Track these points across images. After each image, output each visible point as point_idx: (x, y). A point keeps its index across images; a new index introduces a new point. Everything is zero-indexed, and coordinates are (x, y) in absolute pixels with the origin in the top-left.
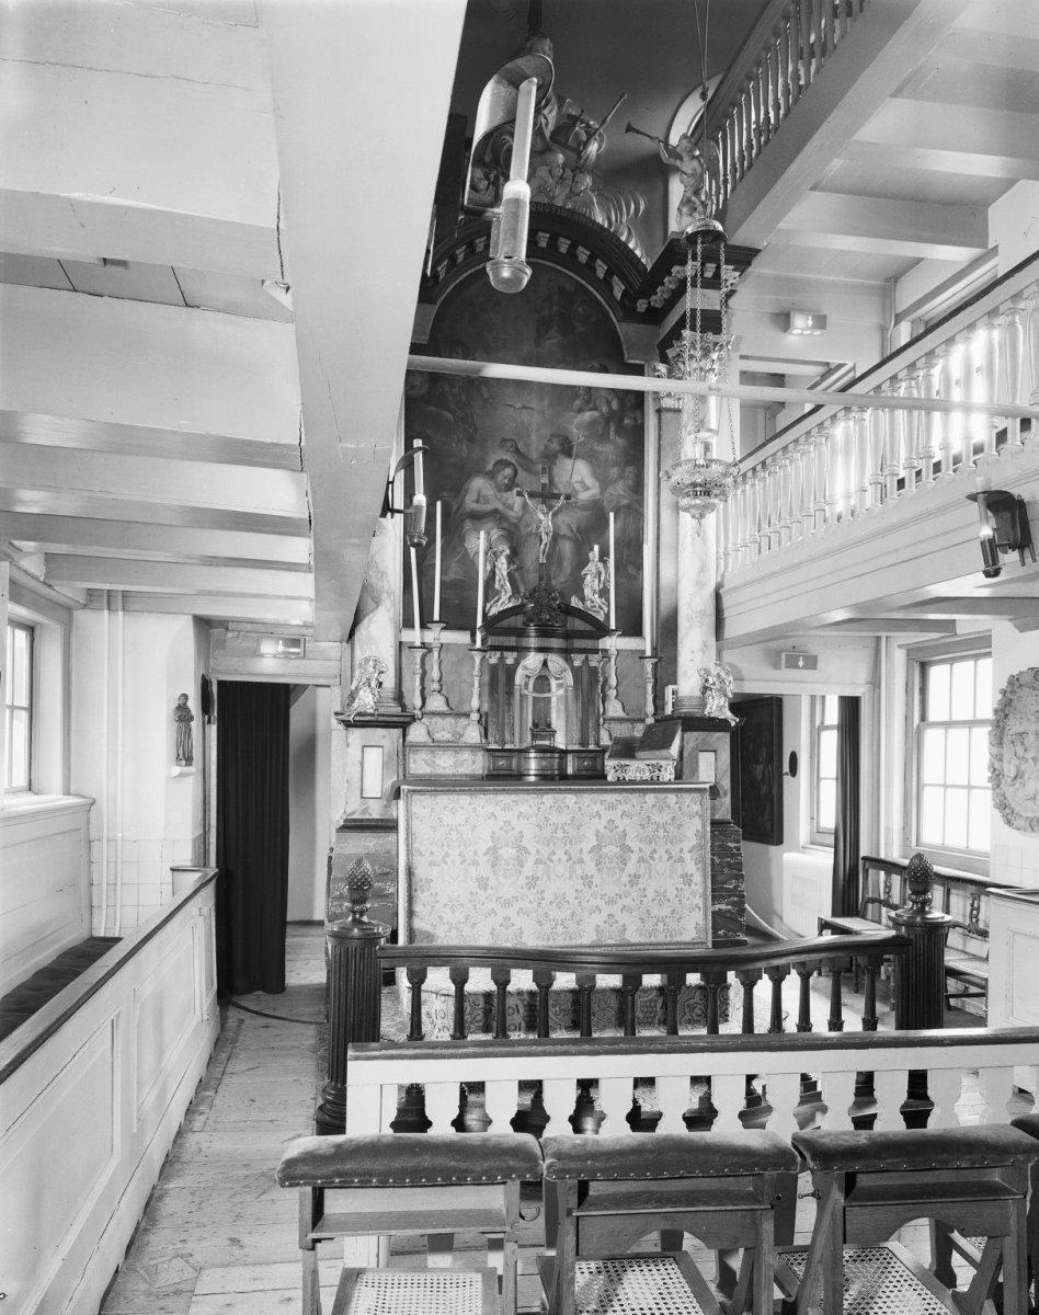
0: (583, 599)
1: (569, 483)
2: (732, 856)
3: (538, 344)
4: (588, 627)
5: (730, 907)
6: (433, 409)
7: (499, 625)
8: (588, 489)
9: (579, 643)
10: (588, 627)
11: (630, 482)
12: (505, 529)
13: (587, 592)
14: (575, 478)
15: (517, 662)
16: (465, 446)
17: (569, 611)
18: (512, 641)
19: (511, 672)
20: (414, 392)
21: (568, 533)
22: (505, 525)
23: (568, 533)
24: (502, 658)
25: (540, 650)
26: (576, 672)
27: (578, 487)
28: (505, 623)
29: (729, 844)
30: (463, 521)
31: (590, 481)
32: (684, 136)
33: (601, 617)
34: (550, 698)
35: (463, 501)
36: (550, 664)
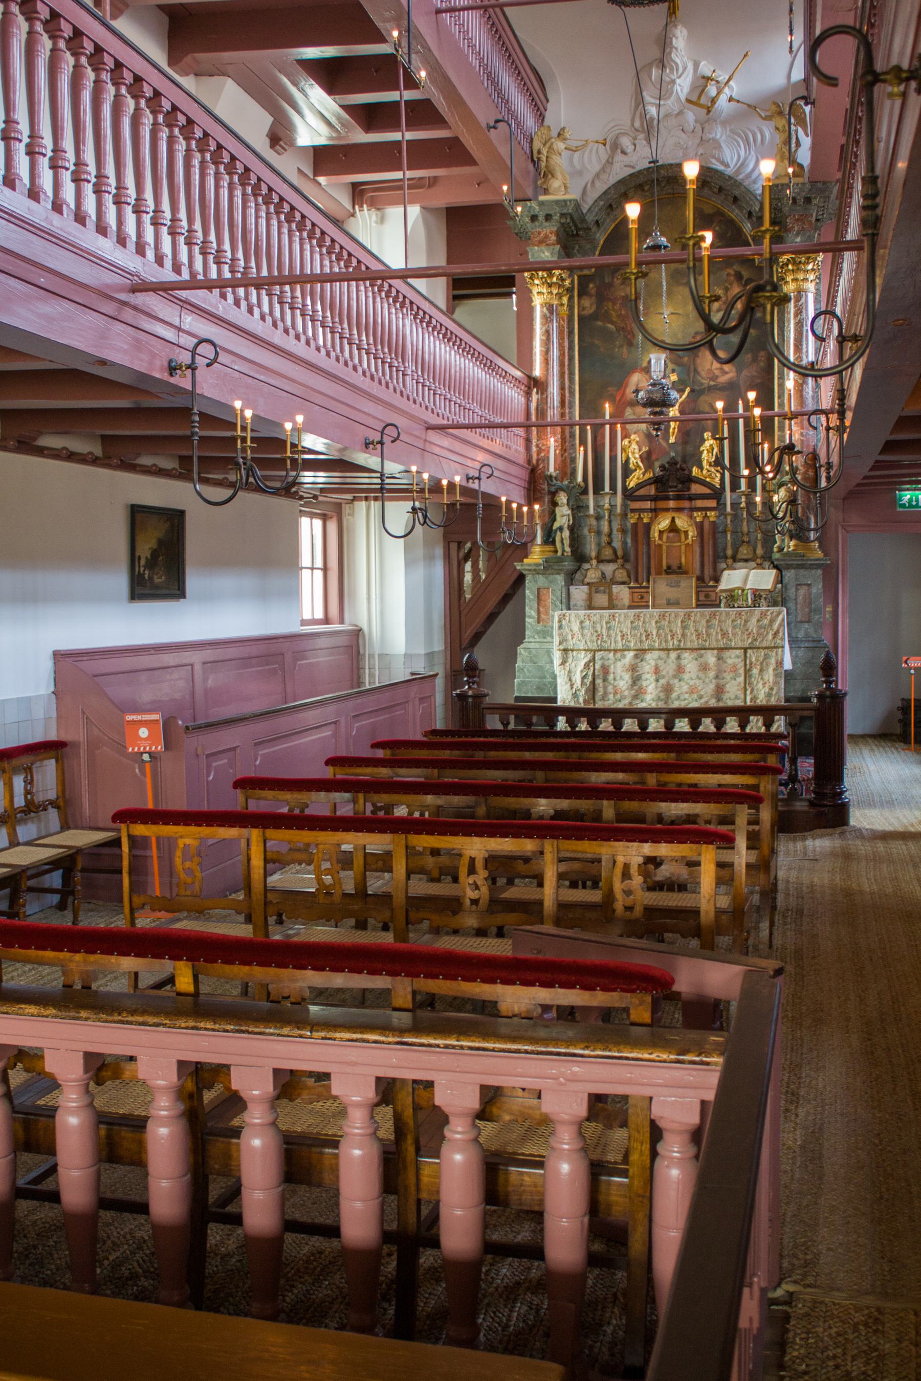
0: (701, 468)
1: (710, 371)
4: (708, 491)
6: (599, 323)
7: (636, 494)
9: (699, 503)
10: (708, 491)
11: (762, 364)
13: (705, 463)
15: (652, 520)
16: (625, 350)
17: (690, 480)
18: (648, 505)
19: (648, 527)
20: (586, 313)
24: (640, 519)
25: (667, 510)
26: (700, 527)
27: (717, 372)
28: (642, 492)
30: (625, 408)
33: (717, 481)
35: (624, 393)
36: (677, 521)
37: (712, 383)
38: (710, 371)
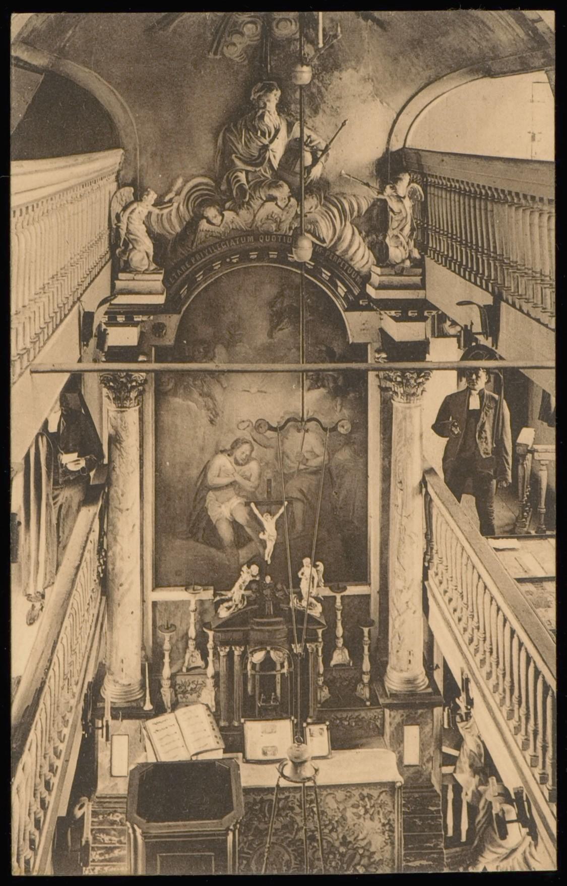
2: (432, 819)
3: (270, 335)
5: (431, 863)
8: (318, 456)
12: (243, 496)
14: (306, 447)
21: (299, 495)
22: (244, 493)
23: (299, 495)
27: (308, 456)
29: (430, 808)
31: (319, 450)
32: (401, 179)
34: (275, 676)
37: (302, 467)
38: (300, 453)
